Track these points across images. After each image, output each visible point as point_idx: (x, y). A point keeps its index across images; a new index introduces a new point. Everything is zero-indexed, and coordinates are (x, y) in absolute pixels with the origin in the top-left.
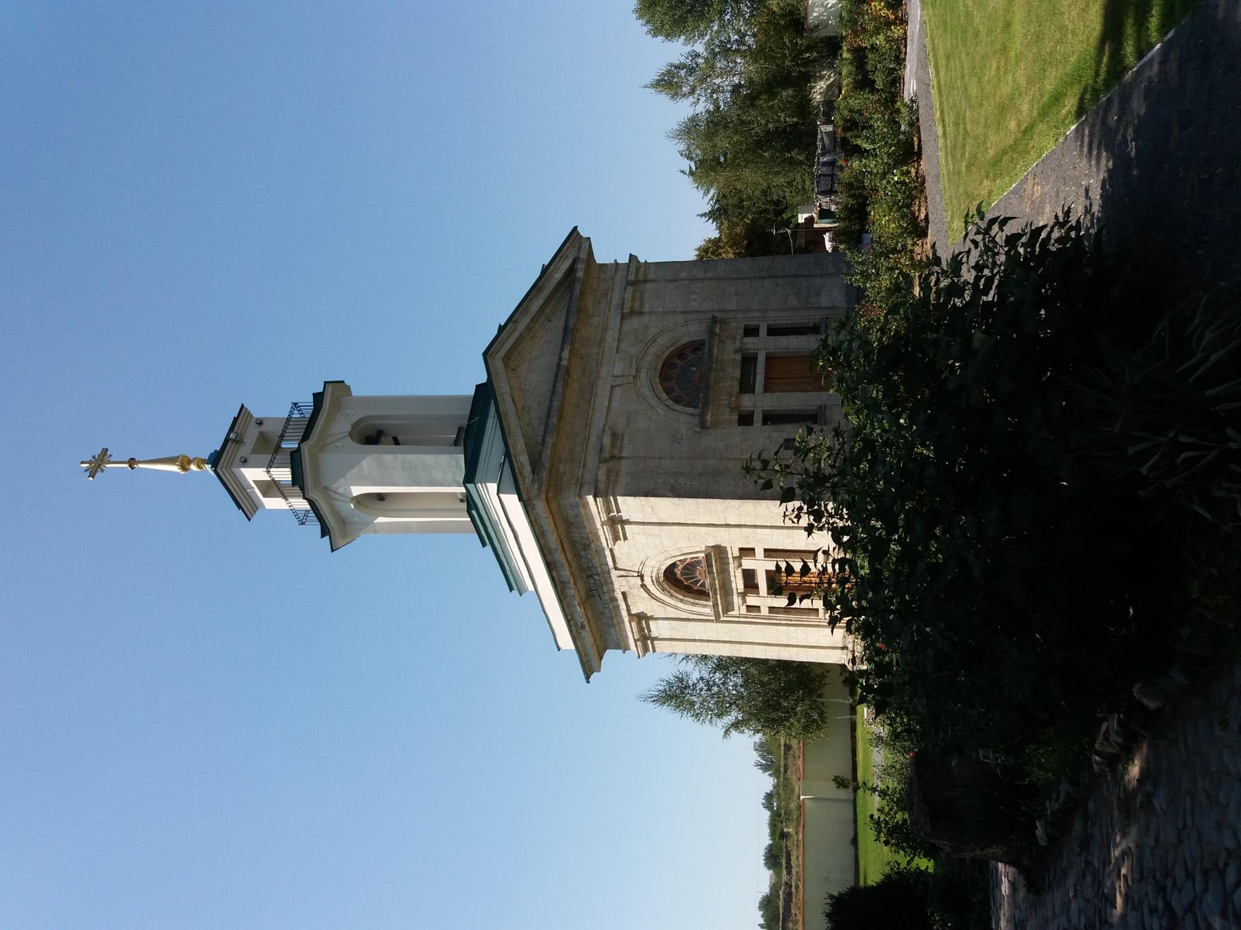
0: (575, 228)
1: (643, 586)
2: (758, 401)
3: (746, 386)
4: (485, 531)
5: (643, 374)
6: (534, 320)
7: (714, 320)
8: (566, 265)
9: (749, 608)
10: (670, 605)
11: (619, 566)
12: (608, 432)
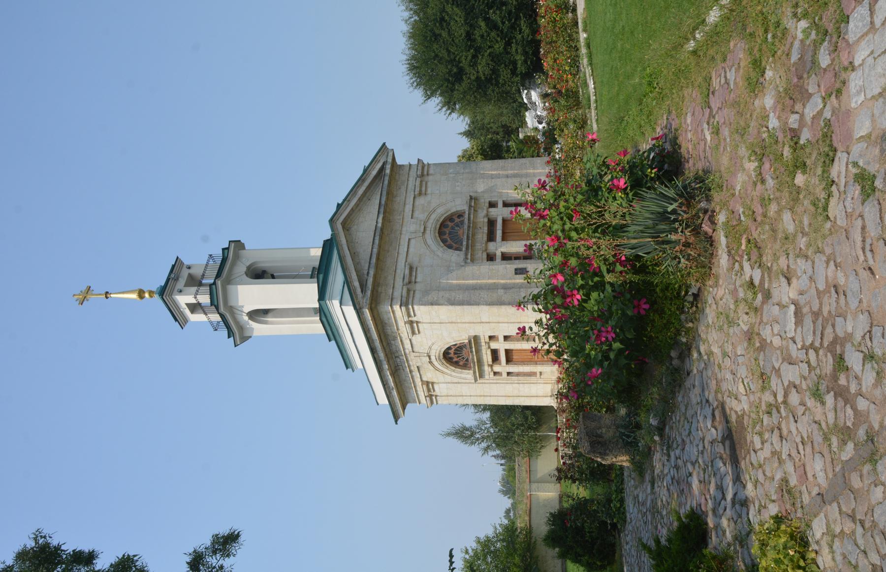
0: (384, 144)
1: (430, 362)
3: (491, 237)
4: (332, 332)
5: (428, 232)
6: (360, 200)
7: (471, 198)
9: (495, 373)
10: (447, 374)
11: (415, 350)
12: (408, 267)
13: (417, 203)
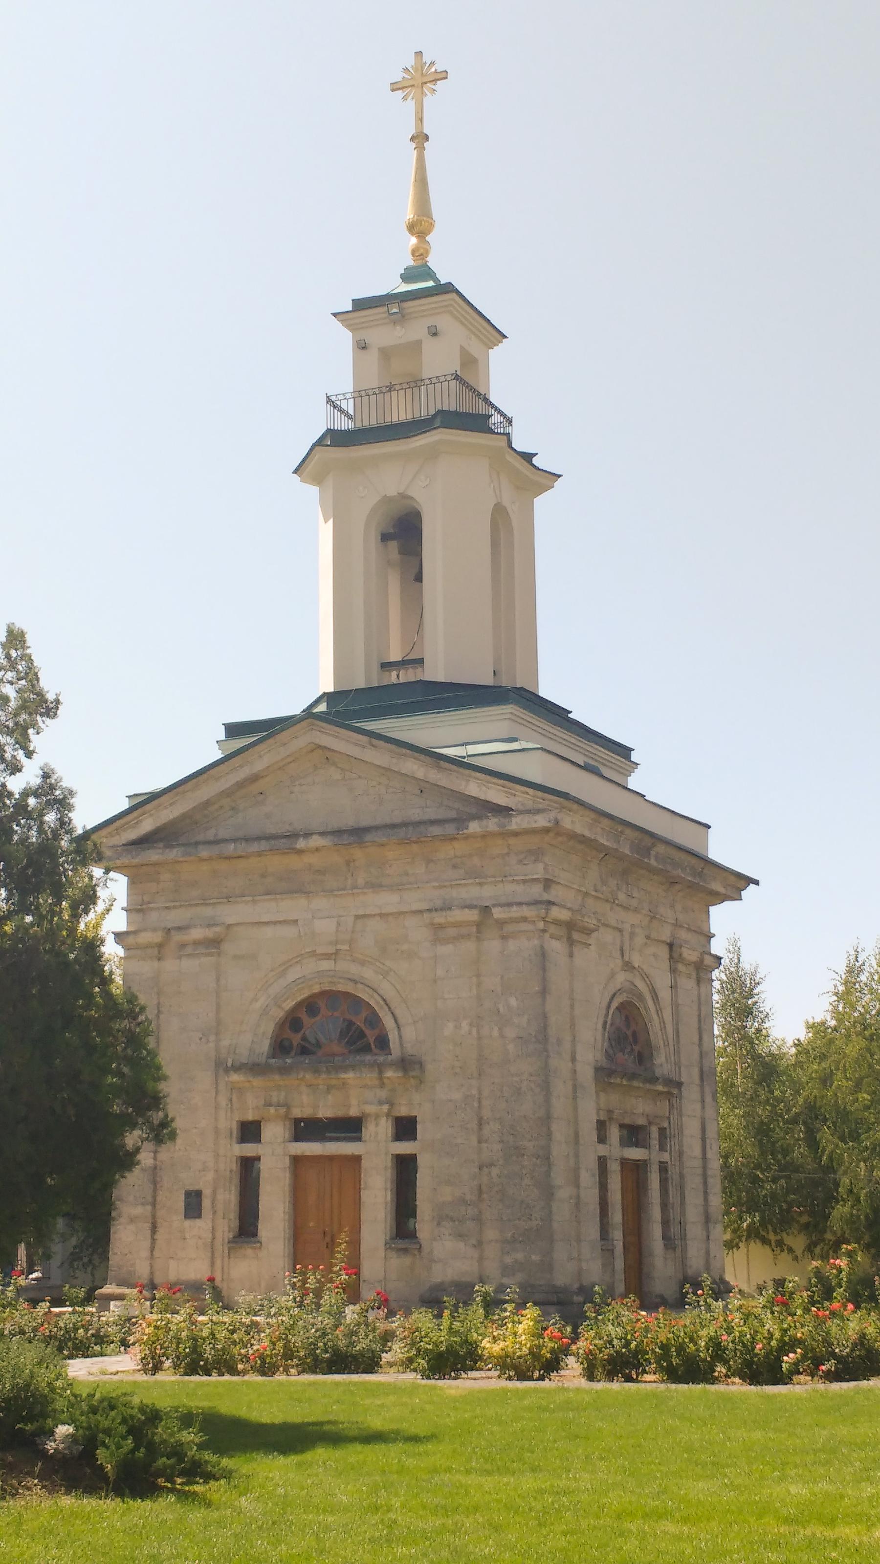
2: (275, 1151)
5: (326, 965)
12: (209, 933)
13: (411, 922)
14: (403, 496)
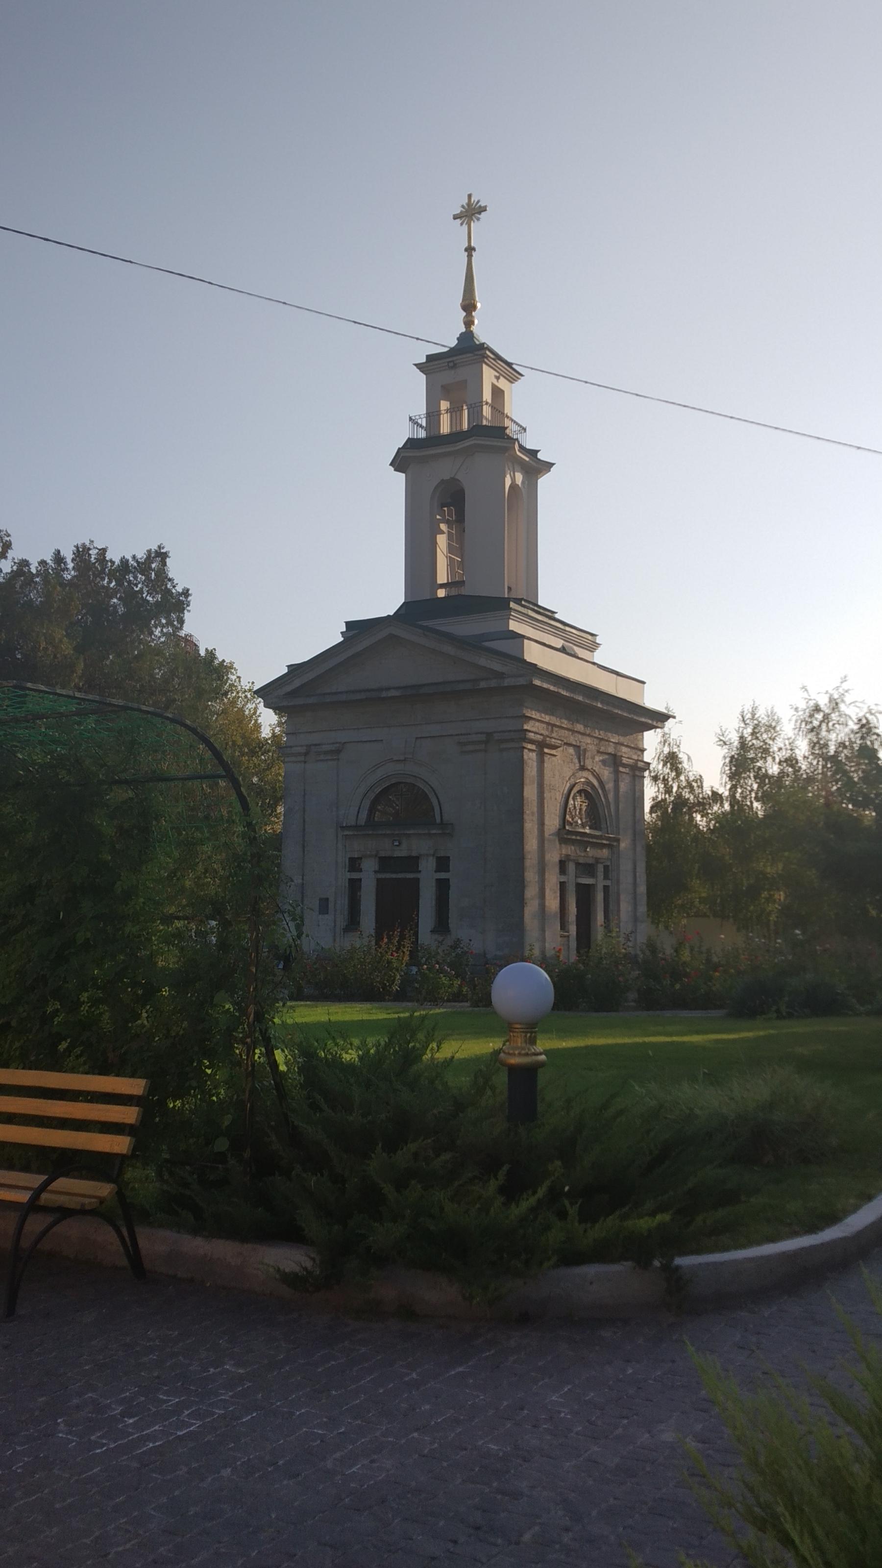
3: (385, 863)
8: (496, 666)
14: (453, 480)
